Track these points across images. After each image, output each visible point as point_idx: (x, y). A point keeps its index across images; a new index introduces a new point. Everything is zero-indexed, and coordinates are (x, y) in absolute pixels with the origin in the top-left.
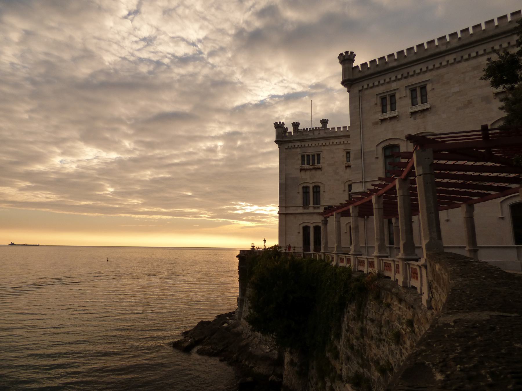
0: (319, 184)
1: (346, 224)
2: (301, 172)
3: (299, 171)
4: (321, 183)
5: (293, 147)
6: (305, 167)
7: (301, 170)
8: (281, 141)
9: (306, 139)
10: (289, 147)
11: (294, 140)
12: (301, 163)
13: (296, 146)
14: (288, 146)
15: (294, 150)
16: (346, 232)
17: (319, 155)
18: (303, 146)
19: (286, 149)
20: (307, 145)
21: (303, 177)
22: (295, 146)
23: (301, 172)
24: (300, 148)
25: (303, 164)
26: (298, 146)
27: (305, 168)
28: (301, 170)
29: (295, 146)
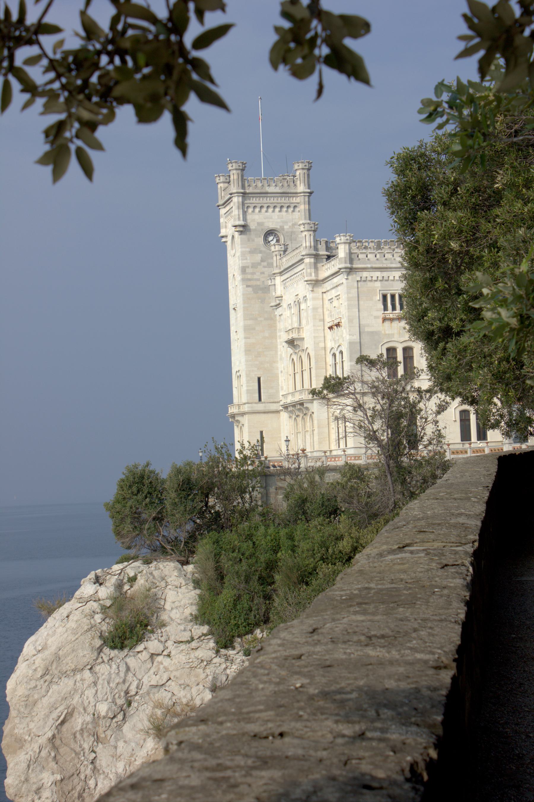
1: (455, 409)
6: (391, 315)
7: (384, 320)
8: (351, 269)
9: (391, 268)
10: (363, 279)
11: (372, 268)
12: (382, 307)
14: (361, 277)
15: (370, 284)
16: (455, 421)
18: (385, 279)
19: (357, 281)
20: (391, 278)
21: (387, 332)
22: (372, 277)
23: (383, 322)
24: (380, 281)
25: (385, 308)
26: (378, 277)
27: (391, 316)
28: (384, 320)
29: (372, 277)
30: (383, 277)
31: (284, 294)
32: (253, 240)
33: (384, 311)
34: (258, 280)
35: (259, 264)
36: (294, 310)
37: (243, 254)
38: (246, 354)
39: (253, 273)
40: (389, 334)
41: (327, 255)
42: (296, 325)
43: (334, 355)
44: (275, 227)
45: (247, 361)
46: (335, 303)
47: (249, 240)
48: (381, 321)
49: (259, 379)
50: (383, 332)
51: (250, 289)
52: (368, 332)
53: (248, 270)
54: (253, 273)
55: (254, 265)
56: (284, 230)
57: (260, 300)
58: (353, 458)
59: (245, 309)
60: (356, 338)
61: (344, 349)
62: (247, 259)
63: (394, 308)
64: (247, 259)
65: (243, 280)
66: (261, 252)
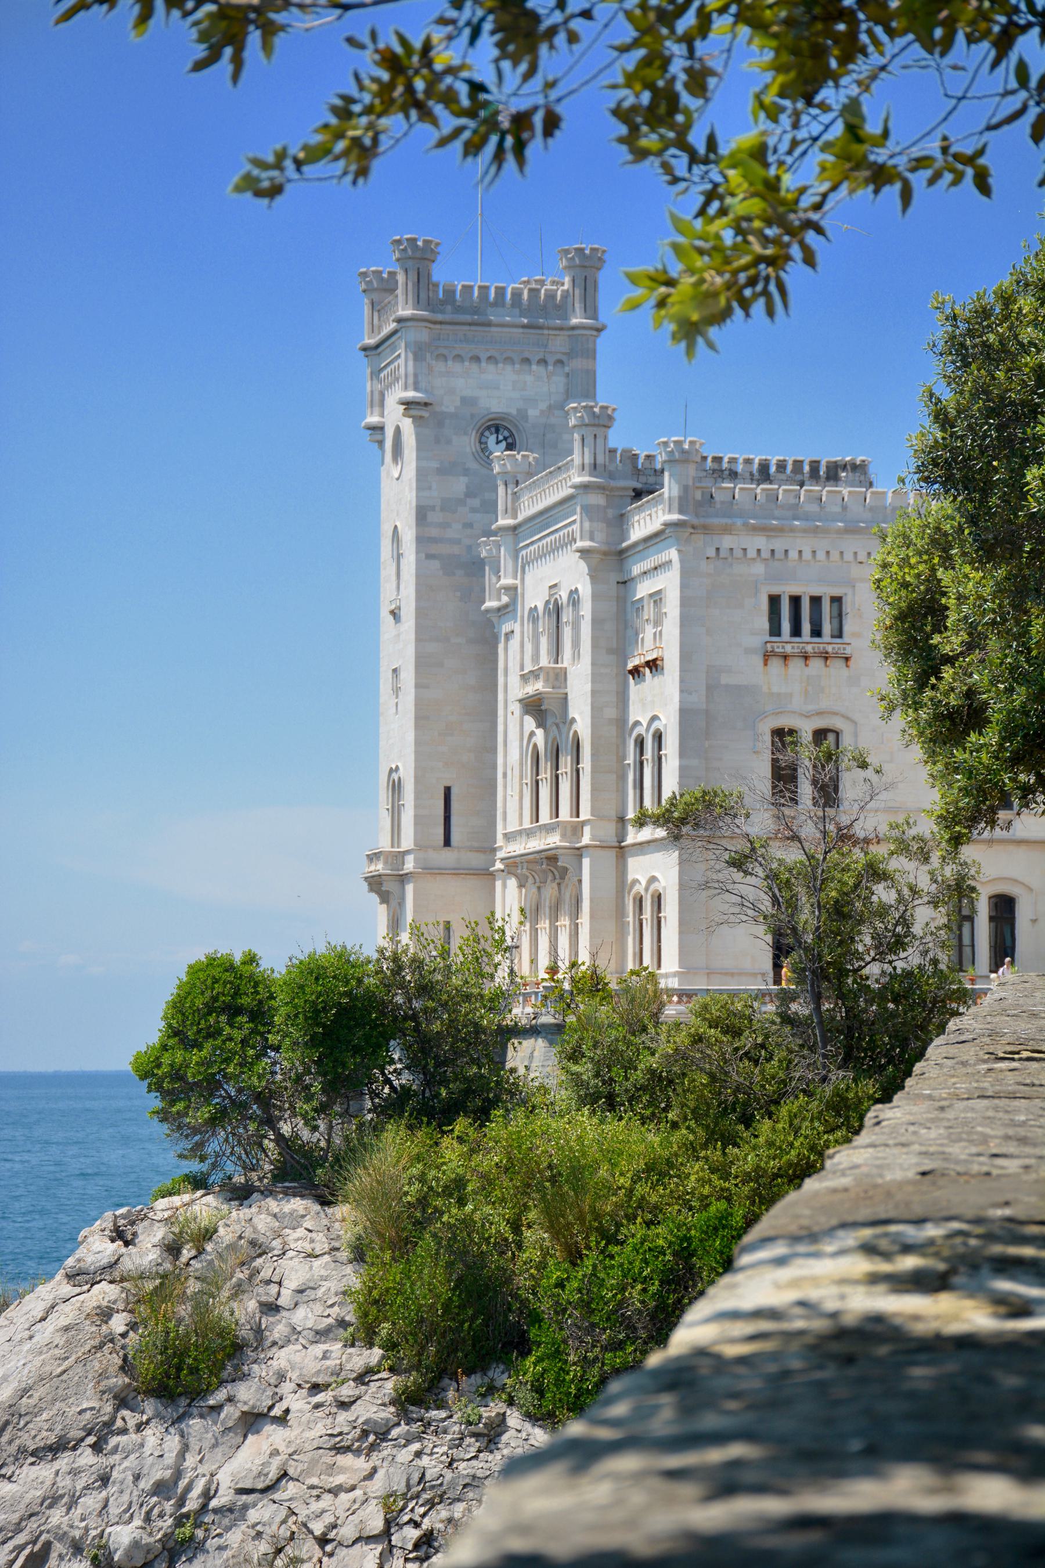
0: (837, 723)
2: (766, 664)
3: (758, 660)
4: (848, 718)
5: (738, 553)
7: (767, 657)
10: (722, 554)
12: (766, 626)
13: (752, 553)
14: (718, 549)
17: (837, 600)
20: (793, 555)
21: (775, 689)
22: (745, 550)
23: (766, 664)
25: (775, 630)
26: (759, 551)
27: (789, 649)
30: (773, 551)
31: (523, 580)
32: (449, 442)
33: (772, 634)
34: (458, 542)
35: (461, 502)
36: (544, 625)
37: (421, 474)
38: (417, 727)
39: (445, 525)
40: (779, 694)
41: (634, 490)
42: (544, 661)
43: (640, 743)
44: (505, 410)
45: (418, 743)
46: (649, 611)
47: (437, 441)
48: (761, 663)
49: (448, 791)
50: (765, 689)
51: (436, 564)
52: (727, 686)
53: (434, 517)
54: (445, 525)
55: (448, 505)
56: (527, 421)
57: (458, 594)
58: (675, 999)
59: (421, 613)
60: (698, 699)
61: (670, 723)
62: (430, 488)
63: (796, 631)
64: (430, 488)
65: (421, 540)
66: (466, 472)
